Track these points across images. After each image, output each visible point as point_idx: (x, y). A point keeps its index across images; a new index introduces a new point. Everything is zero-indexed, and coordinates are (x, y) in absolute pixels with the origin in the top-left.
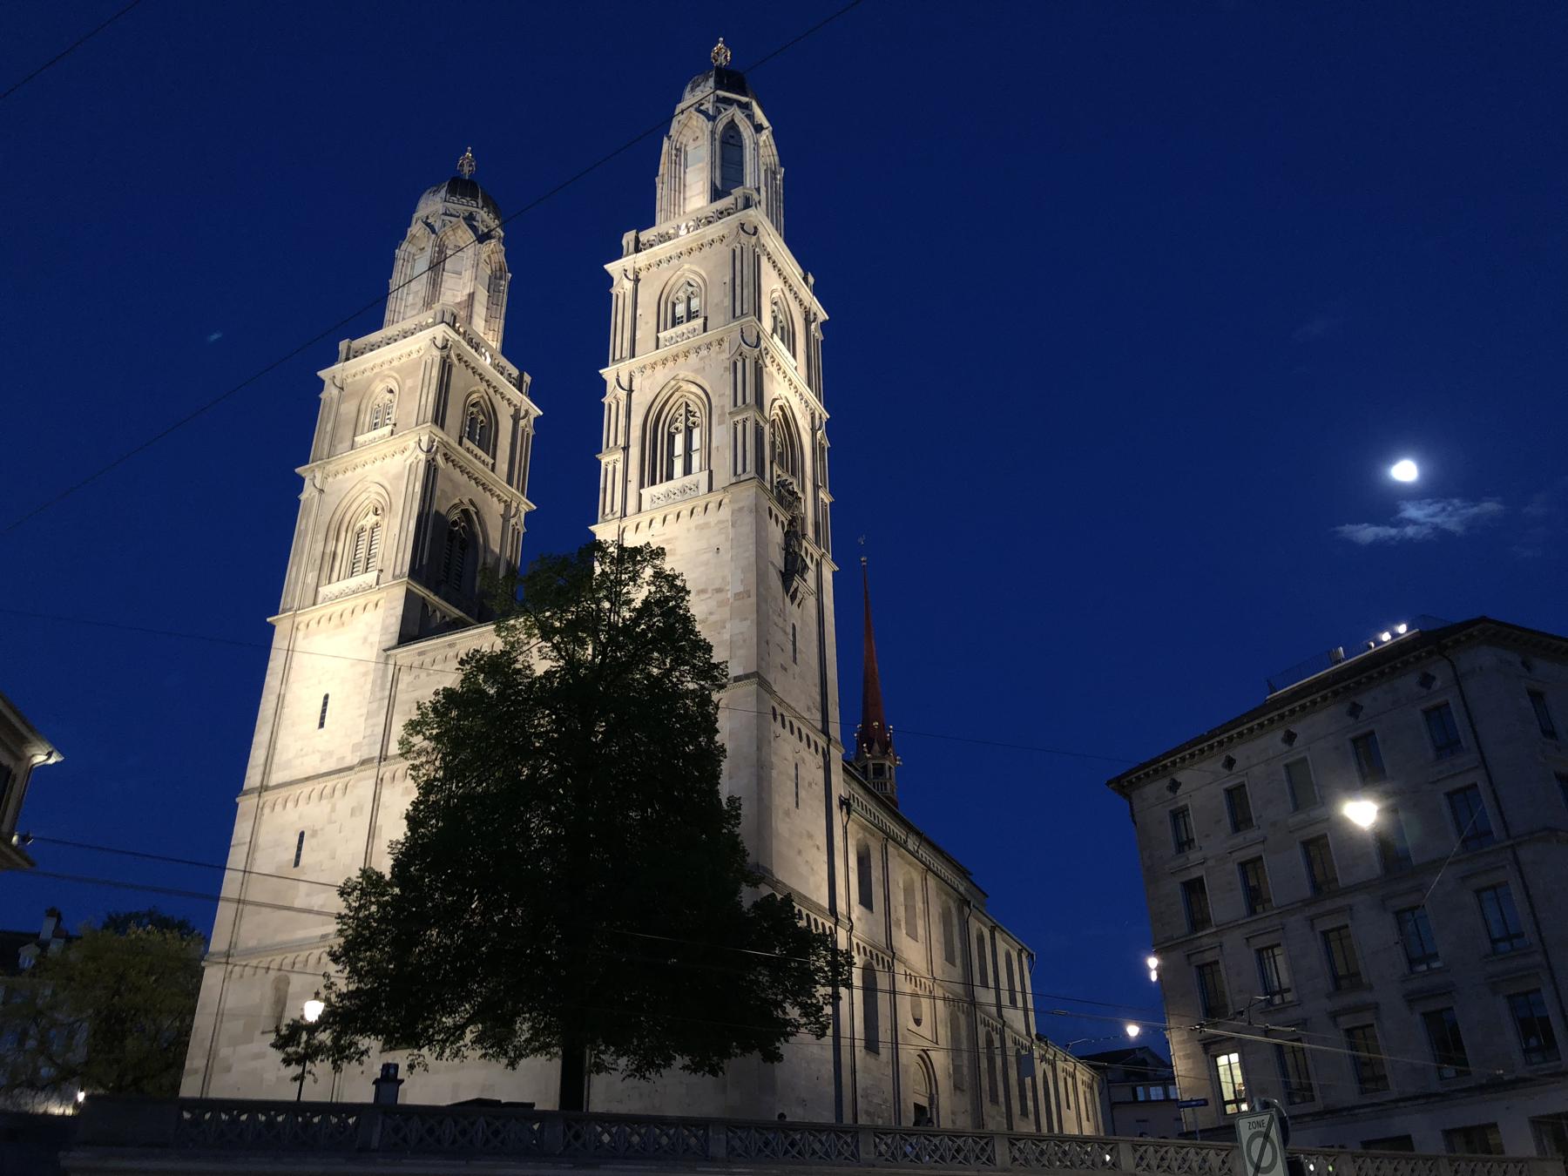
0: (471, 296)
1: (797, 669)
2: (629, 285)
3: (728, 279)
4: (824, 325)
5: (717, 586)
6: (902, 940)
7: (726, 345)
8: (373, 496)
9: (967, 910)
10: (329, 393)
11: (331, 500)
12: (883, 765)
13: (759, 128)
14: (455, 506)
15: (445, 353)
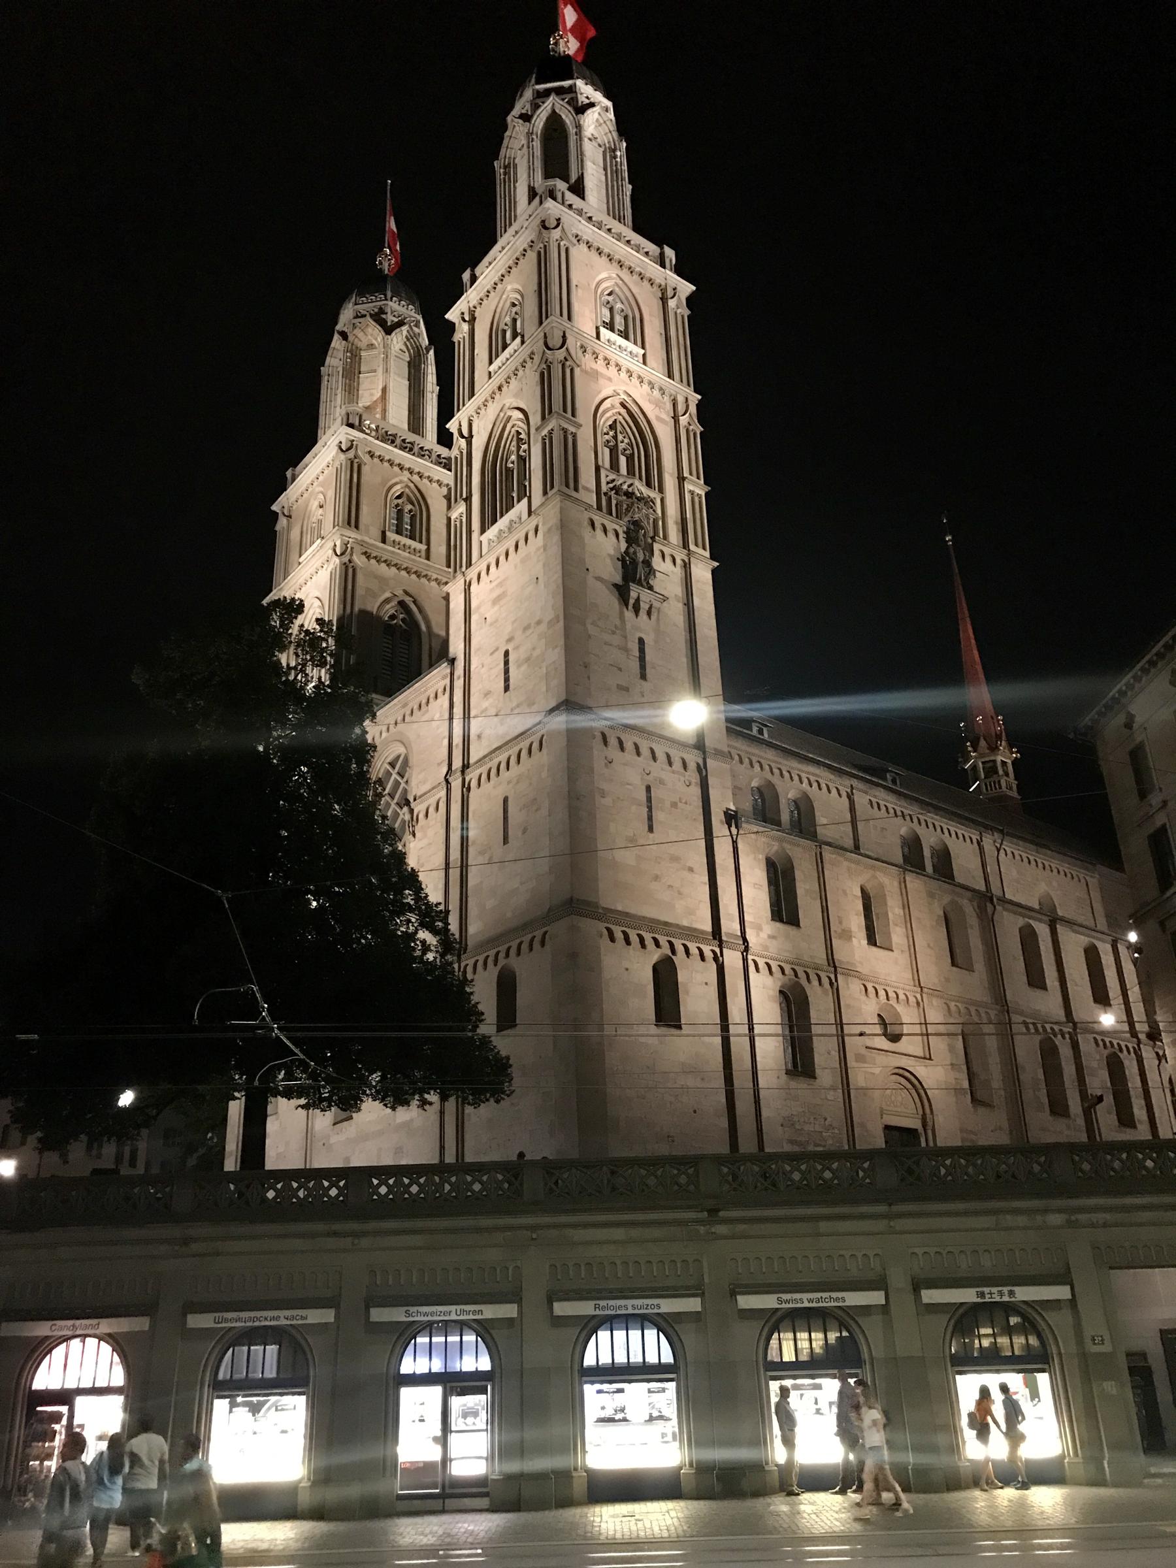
0: (384, 390)
2: (465, 327)
3: (536, 288)
4: (689, 300)
6: (855, 949)
9: (989, 907)
10: (282, 522)
12: (994, 761)
13: (581, 110)
14: (387, 601)
15: (351, 454)
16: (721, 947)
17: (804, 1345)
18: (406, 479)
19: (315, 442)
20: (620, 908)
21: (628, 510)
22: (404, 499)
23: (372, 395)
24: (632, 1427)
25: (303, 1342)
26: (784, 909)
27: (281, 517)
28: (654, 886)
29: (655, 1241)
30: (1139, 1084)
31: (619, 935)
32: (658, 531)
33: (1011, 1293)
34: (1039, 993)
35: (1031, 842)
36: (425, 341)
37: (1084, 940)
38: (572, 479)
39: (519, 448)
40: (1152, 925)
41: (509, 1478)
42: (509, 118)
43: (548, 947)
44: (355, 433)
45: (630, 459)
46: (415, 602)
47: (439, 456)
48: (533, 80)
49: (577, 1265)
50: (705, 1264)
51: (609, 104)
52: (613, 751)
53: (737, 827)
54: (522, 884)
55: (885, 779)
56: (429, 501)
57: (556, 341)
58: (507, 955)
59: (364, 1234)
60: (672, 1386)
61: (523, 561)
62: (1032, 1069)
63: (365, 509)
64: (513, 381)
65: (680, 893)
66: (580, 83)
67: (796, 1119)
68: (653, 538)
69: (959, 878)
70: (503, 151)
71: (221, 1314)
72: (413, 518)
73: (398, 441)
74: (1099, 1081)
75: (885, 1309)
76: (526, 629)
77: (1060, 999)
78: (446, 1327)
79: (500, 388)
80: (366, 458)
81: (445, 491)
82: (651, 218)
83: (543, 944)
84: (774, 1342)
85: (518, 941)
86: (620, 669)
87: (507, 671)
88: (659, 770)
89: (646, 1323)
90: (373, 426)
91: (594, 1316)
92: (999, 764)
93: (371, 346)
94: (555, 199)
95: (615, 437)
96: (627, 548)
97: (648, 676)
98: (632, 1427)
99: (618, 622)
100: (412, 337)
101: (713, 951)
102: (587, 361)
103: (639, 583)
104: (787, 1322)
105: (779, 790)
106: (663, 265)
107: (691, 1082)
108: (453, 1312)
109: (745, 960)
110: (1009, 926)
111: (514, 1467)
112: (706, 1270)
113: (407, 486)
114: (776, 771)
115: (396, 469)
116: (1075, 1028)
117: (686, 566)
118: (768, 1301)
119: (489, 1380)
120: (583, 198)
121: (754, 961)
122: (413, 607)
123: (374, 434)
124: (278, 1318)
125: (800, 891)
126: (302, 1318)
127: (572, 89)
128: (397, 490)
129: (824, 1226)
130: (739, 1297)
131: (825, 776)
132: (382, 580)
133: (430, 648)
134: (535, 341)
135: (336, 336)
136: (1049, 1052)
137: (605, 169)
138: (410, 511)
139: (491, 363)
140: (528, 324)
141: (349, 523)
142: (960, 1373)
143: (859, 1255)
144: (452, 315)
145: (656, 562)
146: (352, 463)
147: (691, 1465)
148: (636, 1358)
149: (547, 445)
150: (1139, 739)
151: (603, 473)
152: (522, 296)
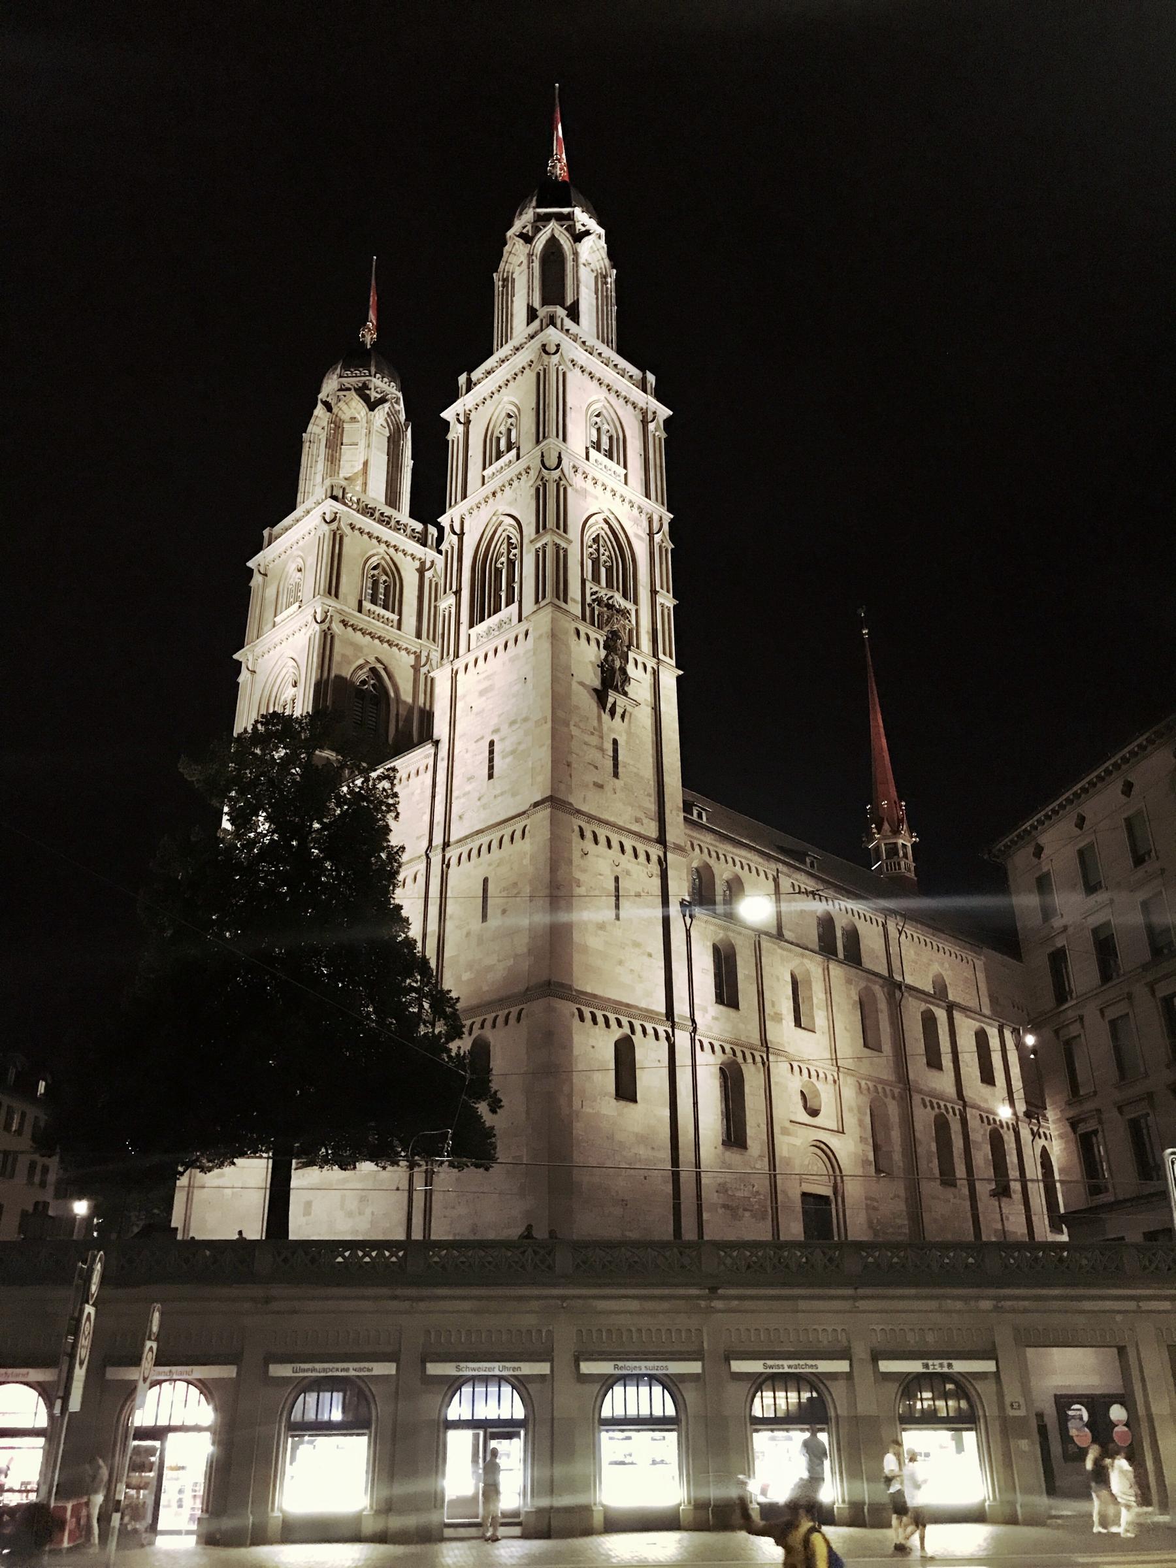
0: (366, 464)
1: (618, 783)
2: (461, 428)
3: (534, 405)
4: (668, 422)
5: (524, 716)
6: (784, 1032)
7: (532, 472)
8: (292, 670)
9: (898, 994)
10: (257, 580)
11: (260, 677)
12: (896, 844)
13: (578, 237)
14: (361, 667)
16: (673, 1028)
17: (781, 1402)
18: (382, 551)
19: (293, 508)
20: (589, 991)
21: (608, 621)
22: (380, 570)
23: (352, 466)
24: (640, 1469)
25: (366, 1390)
26: (727, 994)
27: (255, 571)
28: (619, 969)
29: (664, 1312)
30: (1015, 1160)
31: (588, 1016)
32: (632, 643)
33: (950, 1365)
34: (935, 1073)
35: (929, 926)
36: (402, 417)
37: (976, 1025)
38: (562, 592)
39: (509, 552)
40: (1048, 1032)
41: (540, 1511)
42: (509, 233)
43: (523, 1022)
44: (338, 506)
45: (609, 570)
46: (385, 669)
47: (413, 530)
48: (534, 203)
49: (600, 1330)
50: (705, 1335)
51: (602, 232)
52: (588, 844)
53: (691, 916)
54: (499, 961)
55: (804, 863)
56: (403, 574)
57: (553, 462)
58: (482, 1027)
59: (421, 1299)
60: (673, 1436)
61: (512, 660)
62: (928, 1144)
63: (344, 579)
64: (507, 488)
65: (640, 977)
66: (578, 211)
67: (729, 1185)
68: (629, 647)
69: (867, 963)
70: (502, 264)
71: (298, 1365)
72: (387, 588)
73: (377, 514)
74: (982, 1155)
75: (849, 1376)
76: (513, 723)
77: (953, 1078)
78: (486, 1380)
79: (494, 494)
80: (347, 530)
81: (417, 564)
82: (634, 339)
83: (518, 1020)
84: (757, 1400)
85: (494, 1015)
86: (596, 768)
87: (491, 760)
88: (627, 861)
89: (654, 1382)
90: (355, 499)
91: (612, 1375)
92: (900, 846)
93: (353, 419)
94: (555, 327)
95: (598, 550)
96: (607, 656)
97: (620, 774)
98: (640, 1469)
99: (595, 723)
100: (392, 414)
101: (666, 1032)
102: (577, 481)
103: (616, 689)
104: (769, 1383)
105: (716, 872)
106: (645, 391)
107: (642, 1151)
108: (496, 1368)
109: (693, 1040)
110: (913, 1010)
111: (544, 1502)
112: (705, 1338)
113: (383, 558)
114: (714, 854)
115: (374, 541)
116: (965, 1106)
117: (656, 674)
118: (755, 1366)
119: (520, 1426)
120: (578, 324)
121: (701, 1042)
122: (383, 673)
123: (355, 506)
124: (347, 1370)
125: (740, 976)
126: (369, 1370)
127: (570, 217)
128: (374, 561)
129: (803, 1305)
130: (732, 1362)
131: (755, 860)
132: (358, 648)
133: (397, 715)
134: (531, 456)
135: (320, 405)
136: (942, 1125)
137: (596, 293)
138: (385, 582)
139: (484, 469)
140: (527, 444)
141: (330, 593)
142: (904, 1430)
143: (830, 1329)
144: (448, 414)
145: (630, 668)
146: (335, 534)
147: (689, 1503)
148: (645, 1412)
149: (540, 555)
150: (1045, 870)
151: (588, 585)
152: (519, 410)
